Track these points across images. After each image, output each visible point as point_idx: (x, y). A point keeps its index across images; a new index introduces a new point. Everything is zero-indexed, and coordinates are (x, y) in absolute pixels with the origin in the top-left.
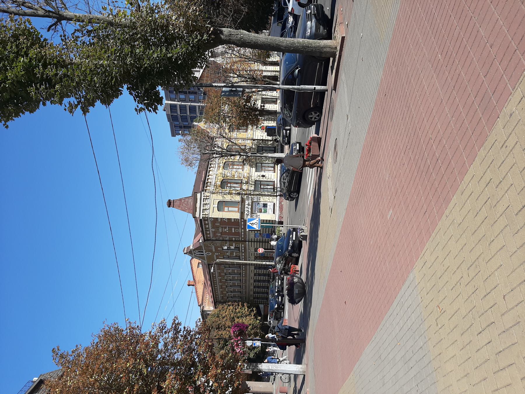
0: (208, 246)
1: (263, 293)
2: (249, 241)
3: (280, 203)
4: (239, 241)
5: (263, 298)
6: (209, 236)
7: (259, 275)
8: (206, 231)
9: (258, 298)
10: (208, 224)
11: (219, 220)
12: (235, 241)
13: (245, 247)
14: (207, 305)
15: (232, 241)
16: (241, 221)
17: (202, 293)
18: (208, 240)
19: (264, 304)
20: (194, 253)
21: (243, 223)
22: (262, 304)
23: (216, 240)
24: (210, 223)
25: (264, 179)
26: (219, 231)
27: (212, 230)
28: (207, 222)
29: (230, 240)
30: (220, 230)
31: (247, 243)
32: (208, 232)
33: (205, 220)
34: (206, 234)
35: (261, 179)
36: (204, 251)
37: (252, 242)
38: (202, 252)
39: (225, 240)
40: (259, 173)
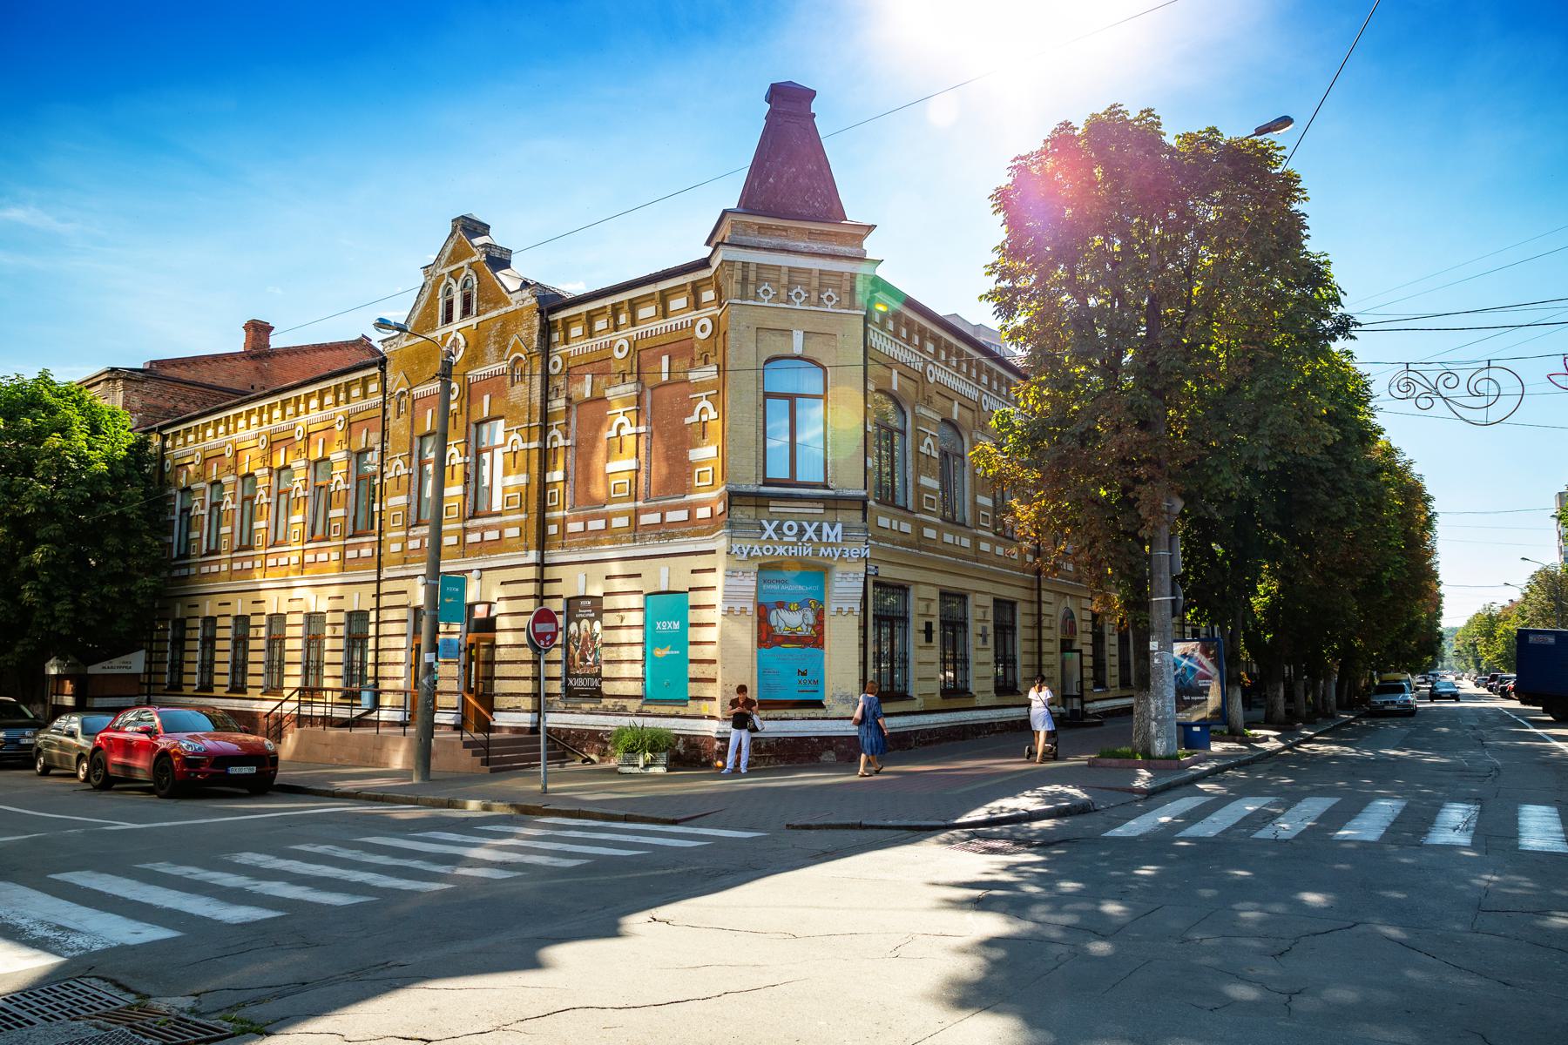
0: (504, 334)
1: (208, 666)
2: (541, 565)
3: (827, 742)
4: (543, 508)
5: (178, 667)
6: (576, 331)
7: (313, 640)
8: (616, 310)
9: (179, 643)
10: (665, 314)
11: (693, 376)
12: (544, 486)
13: (500, 544)
14: (149, 401)
15: (544, 467)
16: (691, 508)
17: (208, 380)
18: (547, 329)
19: (149, 673)
20: (451, 274)
21: (682, 515)
22: (149, 662)
23: (546, 377)
24: (672, 321)
25: (915, 637)
26: (610, 385)
27: (622, 339)
28: (678, 303)
29: (546, 458)
30: (629, 389)
31: (533, 556)
32: (600, 324)
33: (696, 289)
34: (591, 318)
35: (916, 624)
36: (472, 321)
37: (541, 581)
38: (466, 312)
39: (545, 429)
40: (935, 609)
